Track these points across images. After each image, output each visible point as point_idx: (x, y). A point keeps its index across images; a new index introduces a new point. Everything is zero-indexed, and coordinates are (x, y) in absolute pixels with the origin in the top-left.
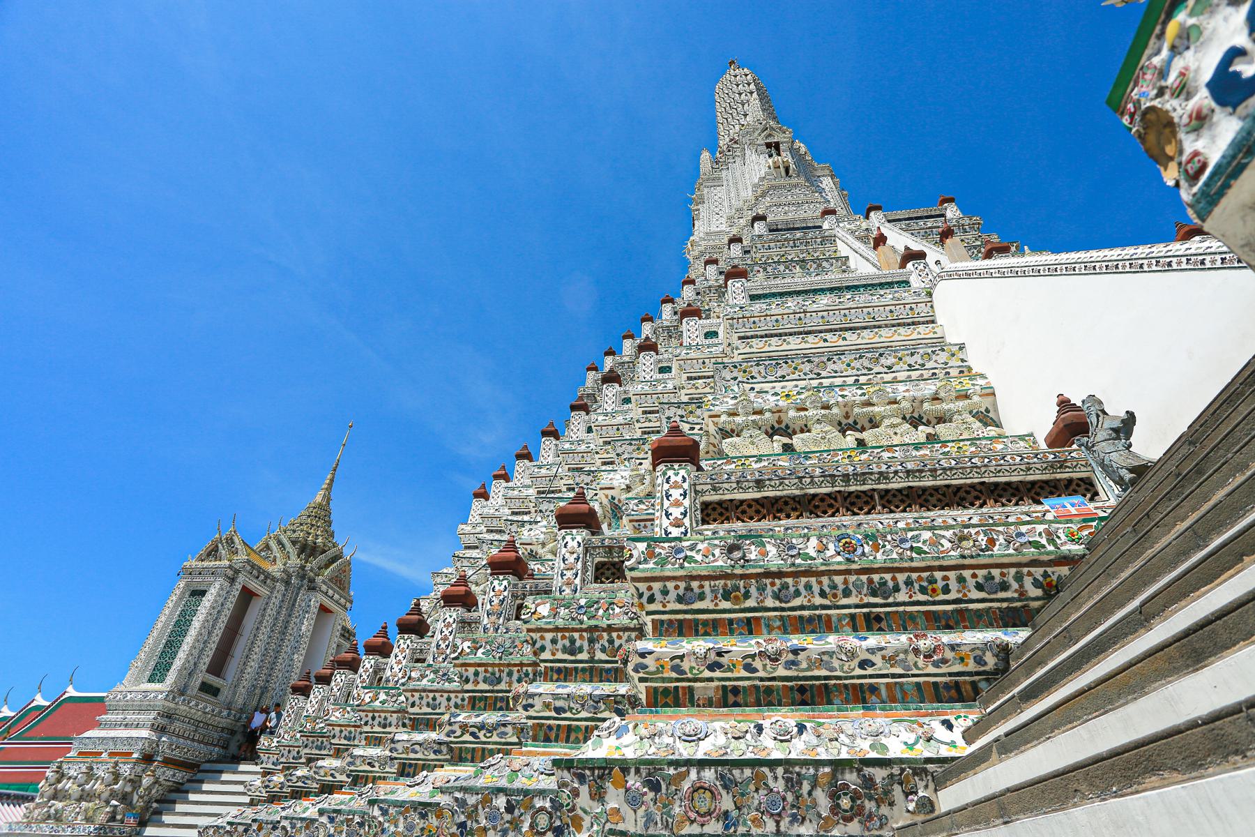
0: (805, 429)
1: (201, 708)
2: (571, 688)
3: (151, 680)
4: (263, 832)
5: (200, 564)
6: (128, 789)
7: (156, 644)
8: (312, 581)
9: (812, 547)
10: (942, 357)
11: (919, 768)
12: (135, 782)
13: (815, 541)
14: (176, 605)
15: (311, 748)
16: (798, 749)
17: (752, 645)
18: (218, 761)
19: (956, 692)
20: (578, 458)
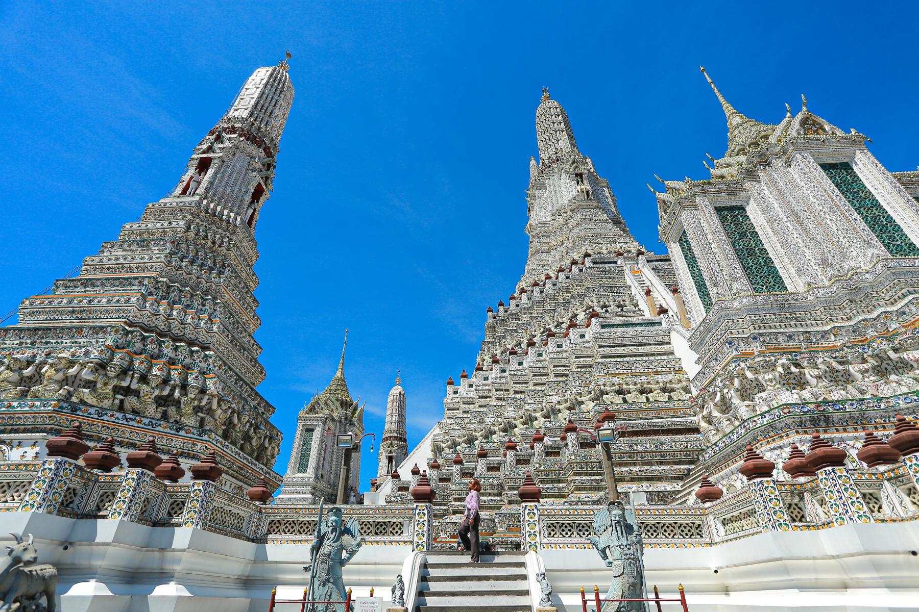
0: (629, 393)
1: (321, 485)
2: (584, 478)
7: (297, 454)
8: (351, 420)
9: (648, 446)
10: (673, 363)
11: (673, 492)
13: (647, 443)
14: (301, 436)
16: (650, 489)
17: (637, 468)
19: (679, 478)
20: (518, 378)
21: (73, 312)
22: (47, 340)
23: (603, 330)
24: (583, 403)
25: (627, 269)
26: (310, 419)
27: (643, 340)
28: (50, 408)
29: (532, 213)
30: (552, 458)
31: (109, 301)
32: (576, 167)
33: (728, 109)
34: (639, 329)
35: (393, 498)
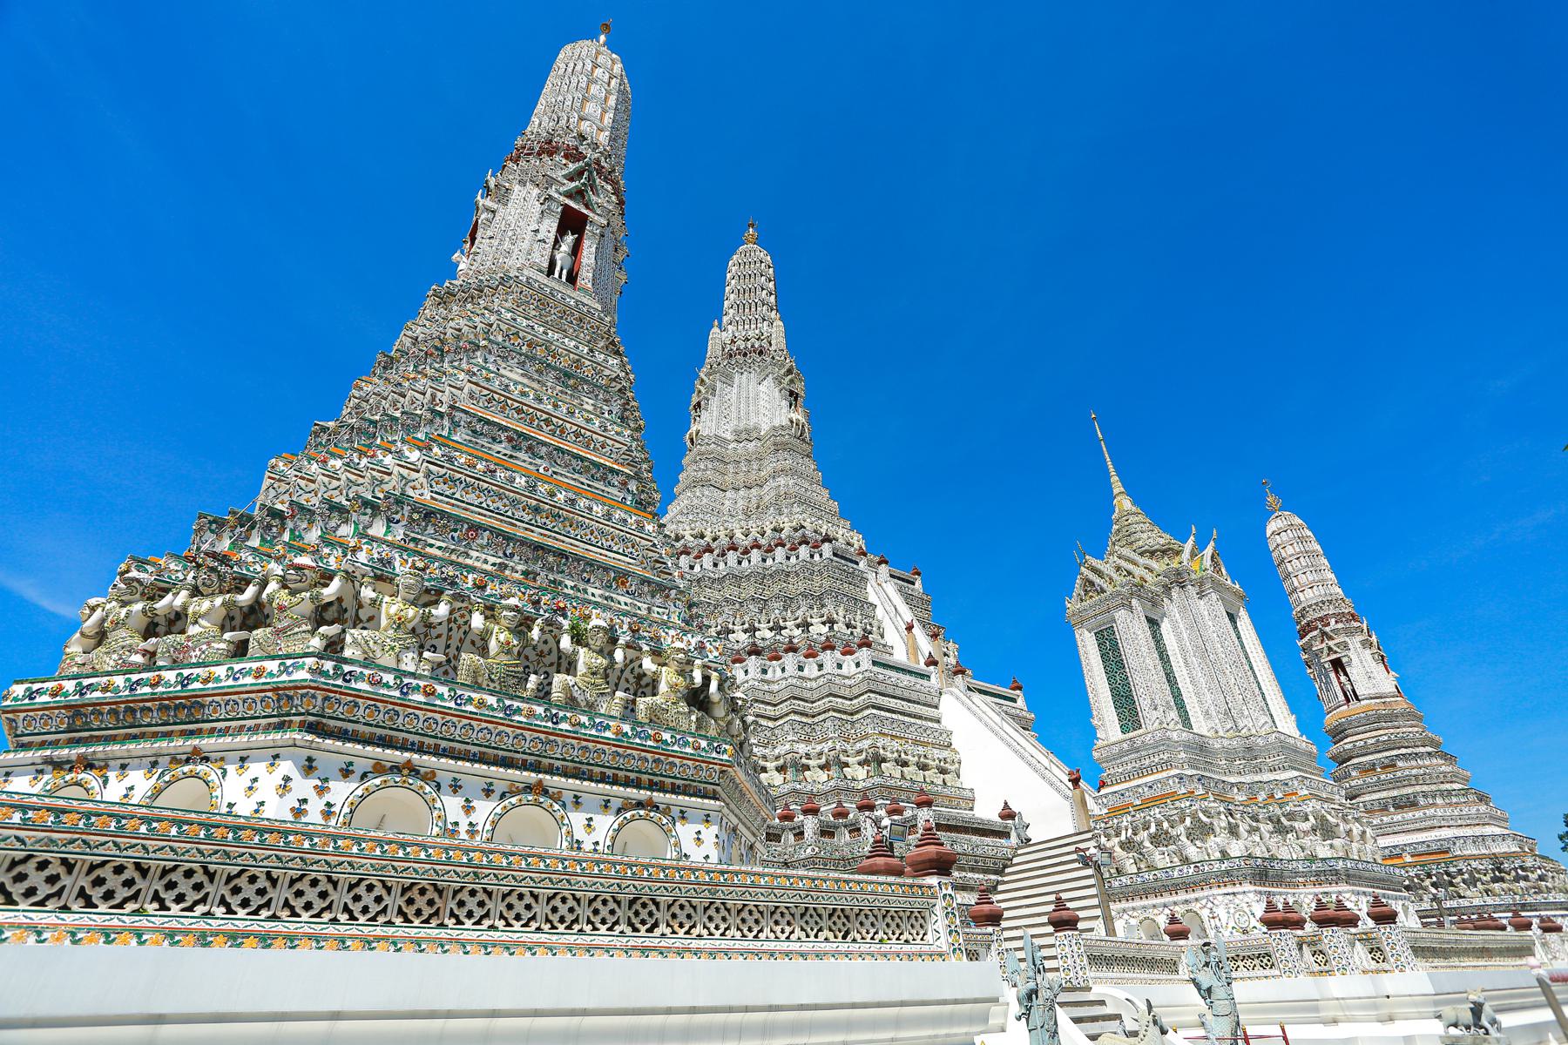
21: (537, 510)
22: (559, 577)
23: (876, 669)
24: (847, 765)
25: (871, 576)
27: (914, 696)
28: (725, 757)
29: (704, 415)
30: (826, 840)
31: (609, 516)
32: (792, 381)
33: (1117, 487)
34: (913, 679)
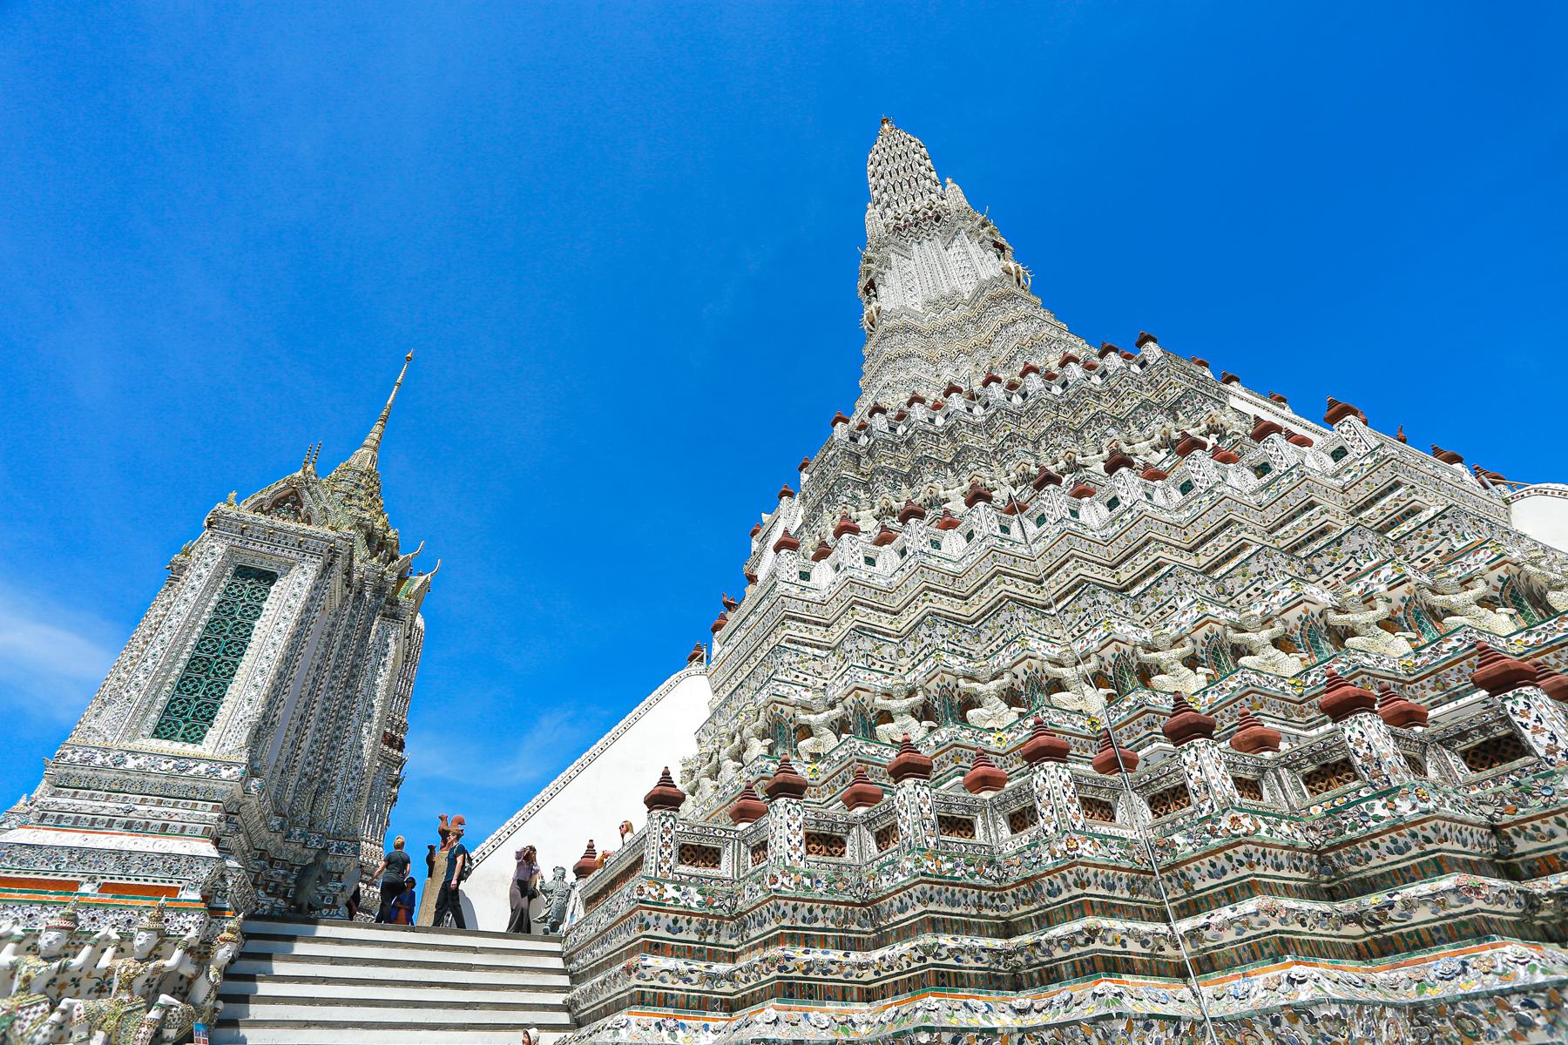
3: (157, 733)
4: (1135, 1034)
5: (264, 520)
6: (189, 970)
8: (394, 602)
12: (200, 953)
14: (210, 587)
15: (939, 903)
18: (283, 918)
26: (271, 535)
35: (670, 892)
